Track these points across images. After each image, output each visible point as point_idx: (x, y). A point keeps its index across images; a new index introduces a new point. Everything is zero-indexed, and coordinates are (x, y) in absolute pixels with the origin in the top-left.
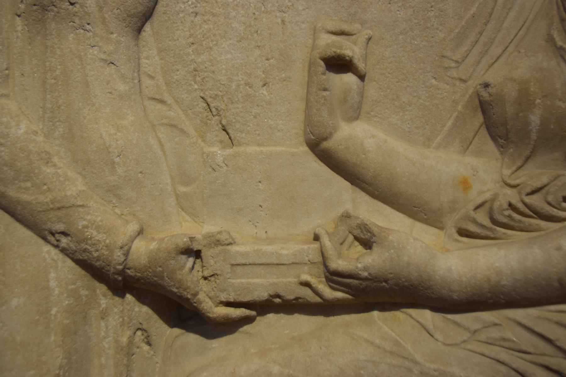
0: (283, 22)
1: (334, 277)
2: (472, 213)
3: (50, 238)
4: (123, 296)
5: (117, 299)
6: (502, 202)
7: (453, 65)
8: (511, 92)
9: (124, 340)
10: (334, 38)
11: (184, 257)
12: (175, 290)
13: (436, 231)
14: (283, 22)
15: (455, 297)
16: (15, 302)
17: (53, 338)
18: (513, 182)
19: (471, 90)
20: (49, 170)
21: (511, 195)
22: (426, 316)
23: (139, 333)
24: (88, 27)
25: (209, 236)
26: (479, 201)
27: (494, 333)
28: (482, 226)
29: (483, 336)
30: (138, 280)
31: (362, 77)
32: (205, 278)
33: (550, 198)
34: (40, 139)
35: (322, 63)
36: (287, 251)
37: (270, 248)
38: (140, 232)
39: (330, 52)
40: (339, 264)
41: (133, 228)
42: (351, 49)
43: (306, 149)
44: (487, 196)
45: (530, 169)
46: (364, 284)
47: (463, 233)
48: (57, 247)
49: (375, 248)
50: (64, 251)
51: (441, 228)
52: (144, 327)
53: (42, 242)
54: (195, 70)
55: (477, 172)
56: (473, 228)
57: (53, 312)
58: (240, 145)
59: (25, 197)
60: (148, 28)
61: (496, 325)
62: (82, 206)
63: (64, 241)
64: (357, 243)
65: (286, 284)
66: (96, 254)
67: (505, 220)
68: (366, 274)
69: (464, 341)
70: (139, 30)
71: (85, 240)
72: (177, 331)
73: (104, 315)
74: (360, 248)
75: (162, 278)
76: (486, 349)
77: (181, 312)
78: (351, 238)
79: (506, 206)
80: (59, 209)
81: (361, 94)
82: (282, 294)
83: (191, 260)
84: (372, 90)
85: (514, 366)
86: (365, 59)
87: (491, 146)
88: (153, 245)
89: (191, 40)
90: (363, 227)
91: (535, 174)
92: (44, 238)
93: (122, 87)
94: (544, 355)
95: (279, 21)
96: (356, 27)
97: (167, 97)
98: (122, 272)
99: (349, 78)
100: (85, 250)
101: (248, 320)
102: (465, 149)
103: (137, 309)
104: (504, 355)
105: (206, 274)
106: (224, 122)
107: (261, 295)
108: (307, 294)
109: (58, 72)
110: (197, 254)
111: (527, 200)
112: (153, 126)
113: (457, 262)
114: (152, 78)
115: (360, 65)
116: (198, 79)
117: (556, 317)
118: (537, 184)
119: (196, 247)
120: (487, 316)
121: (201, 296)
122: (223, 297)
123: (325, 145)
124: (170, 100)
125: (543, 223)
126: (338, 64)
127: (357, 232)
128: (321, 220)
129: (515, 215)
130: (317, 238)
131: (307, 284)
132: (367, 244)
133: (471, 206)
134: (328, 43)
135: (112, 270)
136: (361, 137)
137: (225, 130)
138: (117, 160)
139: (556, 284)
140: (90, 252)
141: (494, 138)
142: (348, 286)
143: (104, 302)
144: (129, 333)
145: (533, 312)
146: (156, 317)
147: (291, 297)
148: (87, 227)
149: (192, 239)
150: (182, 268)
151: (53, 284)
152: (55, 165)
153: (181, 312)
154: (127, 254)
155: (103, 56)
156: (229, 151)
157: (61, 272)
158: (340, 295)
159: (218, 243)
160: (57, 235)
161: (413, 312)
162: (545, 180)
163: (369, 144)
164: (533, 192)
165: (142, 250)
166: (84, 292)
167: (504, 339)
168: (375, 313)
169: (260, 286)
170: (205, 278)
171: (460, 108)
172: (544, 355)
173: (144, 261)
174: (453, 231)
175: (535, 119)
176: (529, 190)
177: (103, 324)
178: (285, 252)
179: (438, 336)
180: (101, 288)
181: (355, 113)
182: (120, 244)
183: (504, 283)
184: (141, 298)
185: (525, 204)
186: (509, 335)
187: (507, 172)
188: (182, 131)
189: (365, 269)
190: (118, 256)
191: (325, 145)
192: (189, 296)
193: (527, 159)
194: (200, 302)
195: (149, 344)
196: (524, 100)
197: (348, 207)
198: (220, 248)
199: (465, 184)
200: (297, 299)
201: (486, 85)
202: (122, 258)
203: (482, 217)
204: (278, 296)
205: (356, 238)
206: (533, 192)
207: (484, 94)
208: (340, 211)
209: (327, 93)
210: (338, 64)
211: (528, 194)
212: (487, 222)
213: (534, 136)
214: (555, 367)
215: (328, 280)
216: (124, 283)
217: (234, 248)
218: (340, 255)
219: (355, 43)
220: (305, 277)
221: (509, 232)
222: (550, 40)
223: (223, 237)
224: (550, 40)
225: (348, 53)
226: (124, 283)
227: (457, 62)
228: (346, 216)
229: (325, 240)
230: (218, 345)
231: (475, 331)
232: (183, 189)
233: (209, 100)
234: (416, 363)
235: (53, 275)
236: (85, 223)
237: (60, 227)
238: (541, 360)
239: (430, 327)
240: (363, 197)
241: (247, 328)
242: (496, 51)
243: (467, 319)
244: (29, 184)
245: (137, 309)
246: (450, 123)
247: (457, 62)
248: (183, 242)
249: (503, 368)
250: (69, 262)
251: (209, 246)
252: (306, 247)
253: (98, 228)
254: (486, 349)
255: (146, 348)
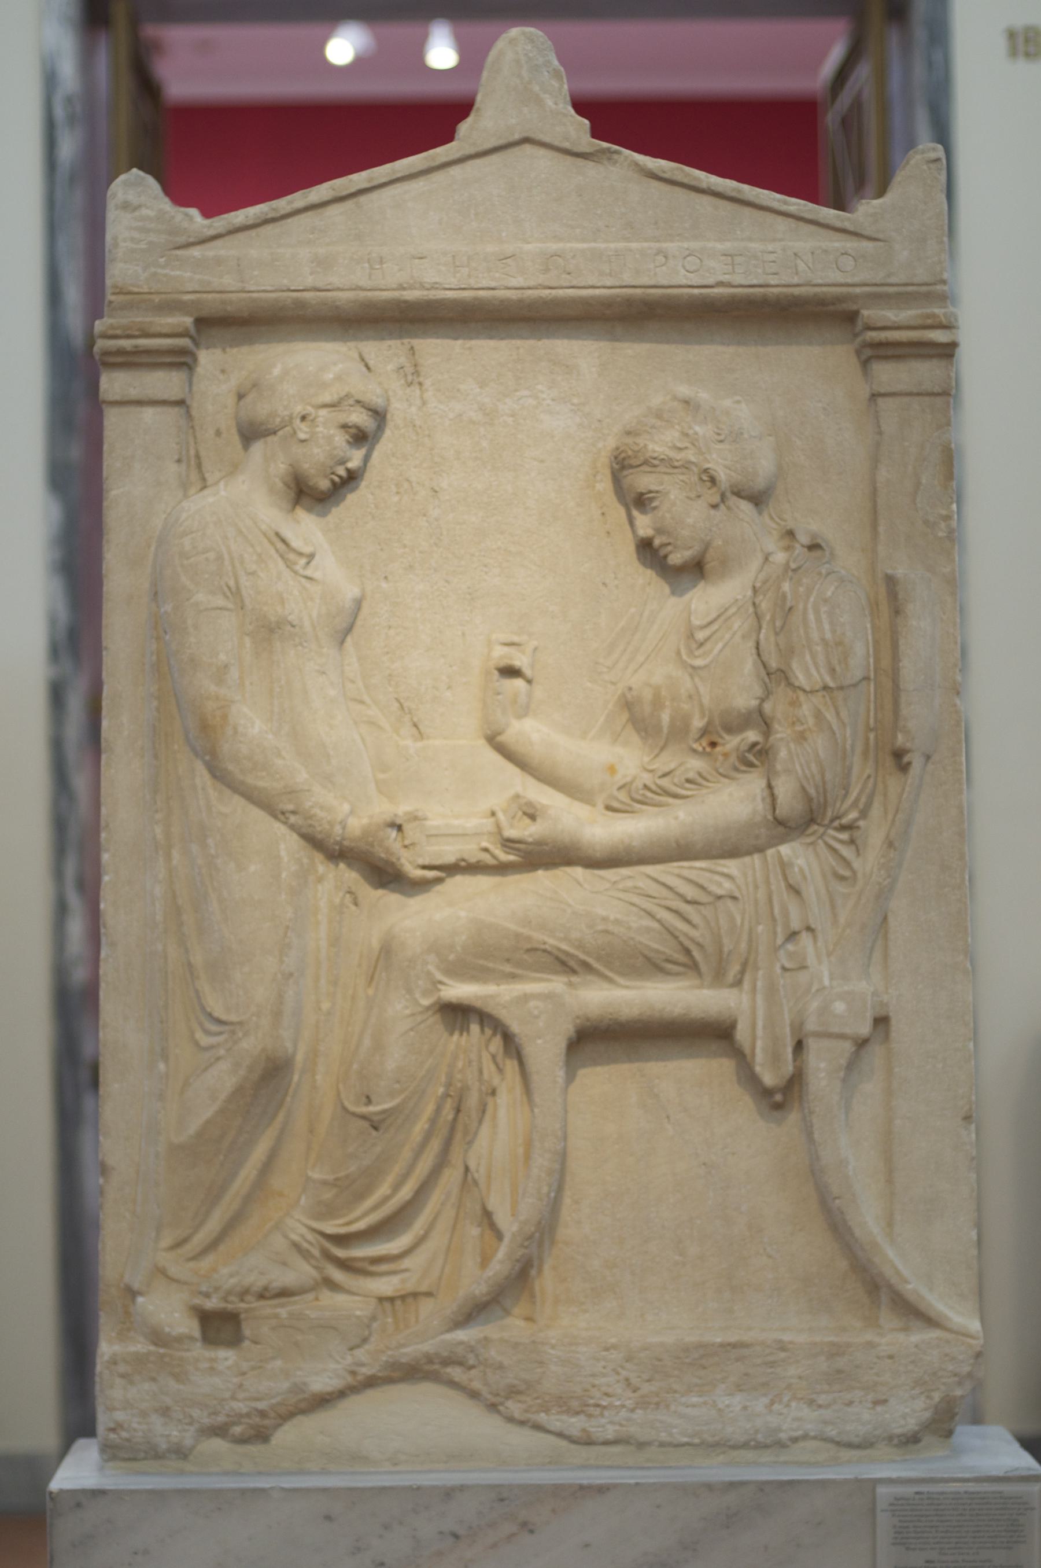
0: (463, 634)
1: (508, 843)
2: (616, 793)
3: (282, 817)
4: (337, 865)
5: (332, 866)
6: (639, 784)
7: (605, 670)
8: (648, 695)
9: (337, 901)
10: (506, 649)
11: (389, 830)
12: (383, 855)
13: (587, 808)
14: (463, 634)
15: (598, 855)
16: (252, 868)
17: (283, 897)
18: (651, 767)
19: (619, 692)
20: (279, 762)
21: (647, 778)
22: (578, 872)
23: (348, 896)
24: (305, 644)
25: (406, 813)
26: (621, 783)
27: (629, 883)
28: (622, 802)
29: (620, 886)
30: (351, 850)
31: (529, 682)
32: (406, 847)
33: (676, 780)
34: (270, 736)
35: (496, 673)
36: (471, 824)
37: (456, 822)
38: (352, 812)
39: (503, 663)
40: (511, 833)
41: (346, 807)
42: (519, 661)
43: (482, 742)
44: (628, 779)
45: (665, 756)
46: (530, 847)
47: (609, 808)
48: (285, 823)
49: (539, 820)
50: (292, 827)
51: (594, 805)
52: (353, 889)
53: (272, 820)
54: (390, 675)
55: (630, 760)
56: (615, 804)
57: (284, 875)
58: (428, 738)
59: (261, 784)
60: (349, 639)
61: (630, 877)
62: (308, 791)
63: (293, 819)
64: (525, 818)
65: (469, 850)
66: (319, 829)
67: (639, 798)
68: (530, 840)
69: (606, 890)
70: (342, 642)
71: (311, 817)
72: (380, 892)
73: (320, 880)
74: (527, 821)
75: (372, 846)
76: (621, 895)
77: (385, 875)
78: (520, 813)
79: (641, 786)
80: (290, 793)
81: (529, 695)
82: (466, 857)
83: (393, 833)
84: (538, 692)
85: (643, 906)
86: (532, 666)
87: (635, 738)
88: (365, 821)
89: (386, 650)
90: (530, 804)
91: (667, 761)
92: (276, 817)
93: (332, 692)
94: (666, 899)
95: (460, 633)
96: (524, 638)
97: (366, 698)
98: (339, 843)
99: (519, 683)
100: (310, 826)
101: (439, 881)
102: (615, 739)
103: (347, 875)
104: (636, 899)
105: (407, 842)
106: (415, 719)
107: (450, 859)
108: (487, 858)
109: (283, 682)
110: (399, 828)
111: (659, 782)
112: (356, 723)
113: (600, 830)
114: (353, 682)
115: (528, 672)
116: (393, 683)
117: (676, 871)
118: (667, 769)
119: (398, 822)
120: (625, 871)
121: (403, 861)
122: (420, 861)
123: (499, 738)
124: (368, 700)
125: (670, 800)
126: (510, 672)
127: (525, 808)
128: (497, 800)
129: (649, 794)
130: (493, 814)
131: (486, 850)
132: (533, 817)
133: (616, 787)
134: (500, 654)
135: (332, 841)
136: (530, 732)
137: (415, 725)
138: (332, 753)
139: (674, 845)
140: (314, 827)
141: (638, 731)
142: (518, 850)
143: (321, 869)
144: (341, 894)
145: (659, 867)
146: (362, 881)
147: (473, 860)
148: (312, 807)
149: (396, 815)
150: (388, 838)
151: (283, 853)
152: (284, 758)
153: (385, 875)
154: (344, 828)
155: (317, 668)
156: (420, 744)
157: (289, 845)
158: (512, 858)
159: (416, 818)
160: (287, 815)
161: (569, 870)
162: (672, 766)
163: (535, 737)
164: (664, 775)
165: (356, 825)
166: (305, 861)
167: (636, 888)
168: (540, 873)
169: (449, 852)
170: (406, 847)
171: (610, 706)
172: (666, 899)
173: (358, 833)
174: (600, 806)
175: (665, 717)
176: (660, 773)
177: (320, 887)
178: (468, 825)
179: (586, 886)
180: (319, 857)
181: (524, 712)
182: (339, 819)
183: (634, 844)
184: (349, 865)
185: (657, 785)
186: (641, 884)
187: (646, 759)
188: (380, 727)
189: (531, 836)
190: (338, 829)
191: (499, 738)
192: (394, 860)
193: (662, 749)
194: (402, 865)
195: (356, 904)
196: (657, 703)
197: (519, 789)
198: (417, 822)
199: (612, 770)
200: (478, 862)
201: (630, 689)
202: (340, 832)
203: (622, 796)
204: (463, 860)
205: (525, 813)
206: (664, 775)
207: (629, 696)
208: (512, 792)
209: (500, 697)
210: (510, 672)
211: (660, 777)
212: (628, 801)
213: (665, 730)
214: (674, 908)
215: (504, 846)
216: (338, 852)
217: (428, 823)
218: (512, 826)
219: (523, 653)
220: (485, 844)
221: (644, 807)
222: (678, 653)
223: (420, 814)
224: (678, 653)
225: (517, 663)
226: (338, 852)
227: (608, 667)
228: (517, 796)
229: (501, 816)
230: (415, 903)
231: (615, 883)
232: (381, 776)
233: (402, 701)
234: (570, 905)
235: (282, 846)
236: (310, 804)
237: (290, 807)
238: (663, 903)
239: (581, 879)
240: (531, 781)
241: (439, 888)
242: (641, 658)
243: (610, 874)
244: (264, 774)
245: (347, 875)
246: (602, 719)
247: (608, 667)
248: (388, 818)
249: (634, 909)
250: (295, 836)
251: (409, 821)
252: (485, 821)
253: (322, 808)
254: (621, 895)
255: (353, 908)
